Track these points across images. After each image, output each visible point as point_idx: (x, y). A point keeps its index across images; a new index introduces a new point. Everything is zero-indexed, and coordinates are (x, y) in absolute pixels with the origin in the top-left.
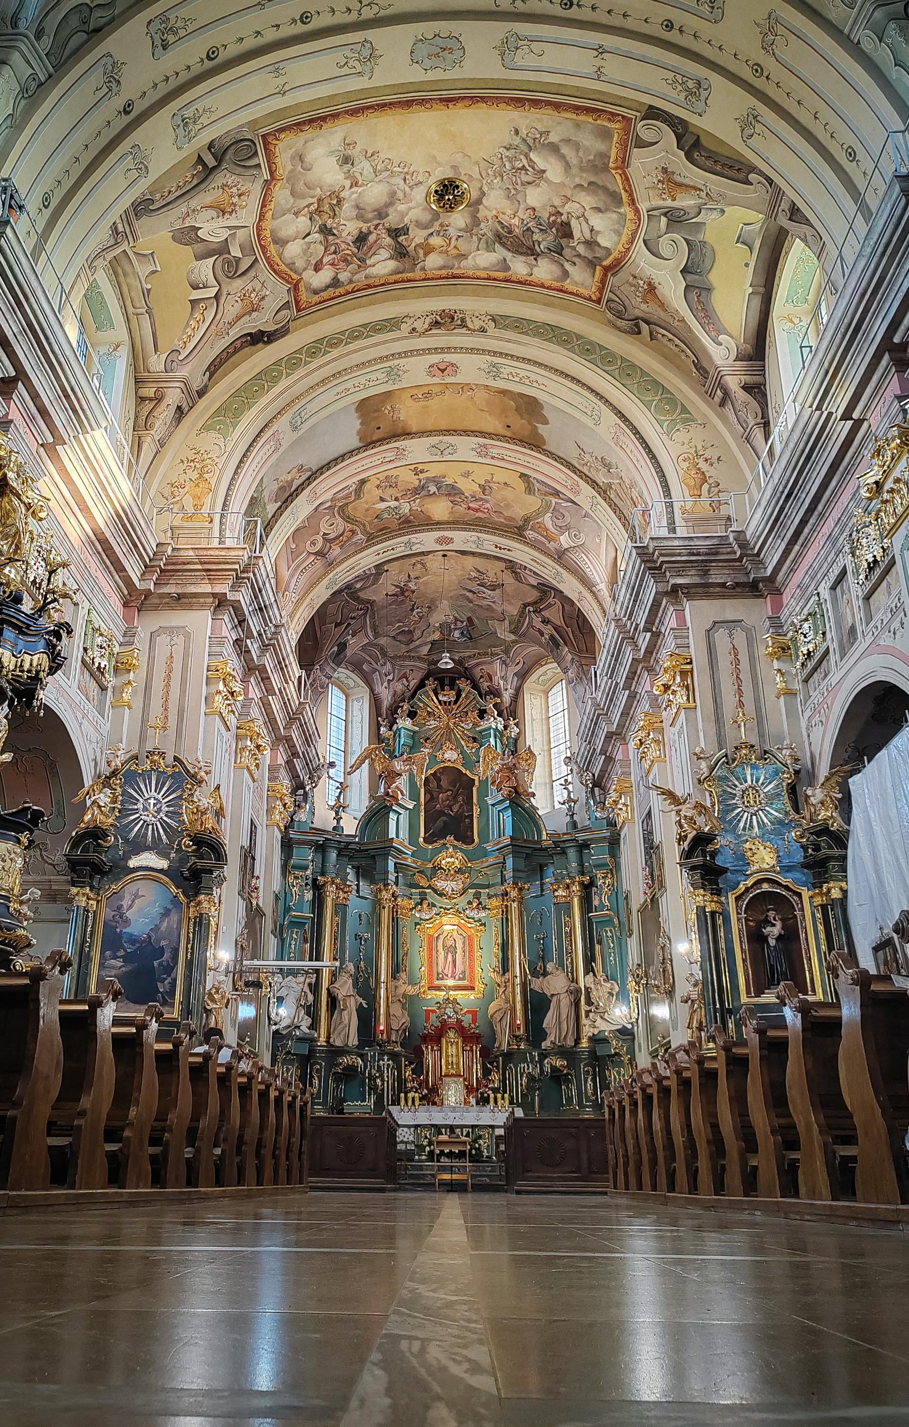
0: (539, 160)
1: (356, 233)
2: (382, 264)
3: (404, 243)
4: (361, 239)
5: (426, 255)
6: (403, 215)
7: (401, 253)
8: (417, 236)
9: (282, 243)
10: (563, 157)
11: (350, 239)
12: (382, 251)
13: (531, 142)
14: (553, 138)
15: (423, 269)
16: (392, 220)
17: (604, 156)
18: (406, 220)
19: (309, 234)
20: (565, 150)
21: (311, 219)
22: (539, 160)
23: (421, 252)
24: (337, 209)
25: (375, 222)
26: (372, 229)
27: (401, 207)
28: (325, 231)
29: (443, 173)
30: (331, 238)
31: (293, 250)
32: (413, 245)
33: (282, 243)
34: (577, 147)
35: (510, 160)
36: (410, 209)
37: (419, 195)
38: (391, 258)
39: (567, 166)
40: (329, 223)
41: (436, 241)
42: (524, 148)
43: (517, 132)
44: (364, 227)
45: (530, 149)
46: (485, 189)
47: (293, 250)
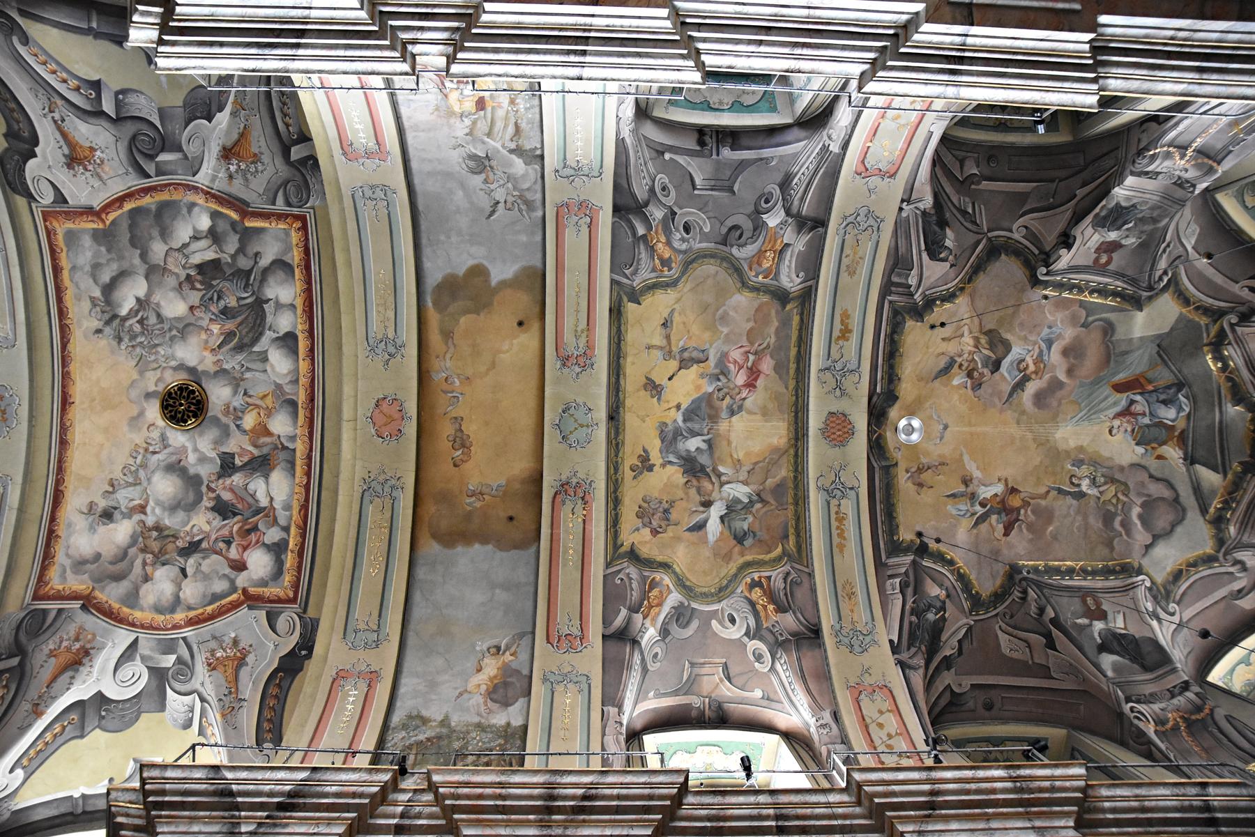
3: (246, 459)
4: (223, 510)
7: (261, 465)
8: (238, 444)
11: (217, 522)
12: (251, 487)
13: (107, 316)
14: (97, 293)
15: (293, 438)
16: (206, 471)
19: (183, 571)
20: (106, 277)
21: (164, 564)
24: (166, 533)
25: (204, 489)
26: (212, 495)
27: (192, 458)
28: (193, 548)
30: (204, 545)
32: (251, 448)
34: (96, 267)
35: (133, 337)
36: (196, 450)
37: (178, 438)
38: (267, 477)
40: (180, 544)
41: (249, 421)
44: (207, 503)
45: (115, 316)
46: (173, 363)
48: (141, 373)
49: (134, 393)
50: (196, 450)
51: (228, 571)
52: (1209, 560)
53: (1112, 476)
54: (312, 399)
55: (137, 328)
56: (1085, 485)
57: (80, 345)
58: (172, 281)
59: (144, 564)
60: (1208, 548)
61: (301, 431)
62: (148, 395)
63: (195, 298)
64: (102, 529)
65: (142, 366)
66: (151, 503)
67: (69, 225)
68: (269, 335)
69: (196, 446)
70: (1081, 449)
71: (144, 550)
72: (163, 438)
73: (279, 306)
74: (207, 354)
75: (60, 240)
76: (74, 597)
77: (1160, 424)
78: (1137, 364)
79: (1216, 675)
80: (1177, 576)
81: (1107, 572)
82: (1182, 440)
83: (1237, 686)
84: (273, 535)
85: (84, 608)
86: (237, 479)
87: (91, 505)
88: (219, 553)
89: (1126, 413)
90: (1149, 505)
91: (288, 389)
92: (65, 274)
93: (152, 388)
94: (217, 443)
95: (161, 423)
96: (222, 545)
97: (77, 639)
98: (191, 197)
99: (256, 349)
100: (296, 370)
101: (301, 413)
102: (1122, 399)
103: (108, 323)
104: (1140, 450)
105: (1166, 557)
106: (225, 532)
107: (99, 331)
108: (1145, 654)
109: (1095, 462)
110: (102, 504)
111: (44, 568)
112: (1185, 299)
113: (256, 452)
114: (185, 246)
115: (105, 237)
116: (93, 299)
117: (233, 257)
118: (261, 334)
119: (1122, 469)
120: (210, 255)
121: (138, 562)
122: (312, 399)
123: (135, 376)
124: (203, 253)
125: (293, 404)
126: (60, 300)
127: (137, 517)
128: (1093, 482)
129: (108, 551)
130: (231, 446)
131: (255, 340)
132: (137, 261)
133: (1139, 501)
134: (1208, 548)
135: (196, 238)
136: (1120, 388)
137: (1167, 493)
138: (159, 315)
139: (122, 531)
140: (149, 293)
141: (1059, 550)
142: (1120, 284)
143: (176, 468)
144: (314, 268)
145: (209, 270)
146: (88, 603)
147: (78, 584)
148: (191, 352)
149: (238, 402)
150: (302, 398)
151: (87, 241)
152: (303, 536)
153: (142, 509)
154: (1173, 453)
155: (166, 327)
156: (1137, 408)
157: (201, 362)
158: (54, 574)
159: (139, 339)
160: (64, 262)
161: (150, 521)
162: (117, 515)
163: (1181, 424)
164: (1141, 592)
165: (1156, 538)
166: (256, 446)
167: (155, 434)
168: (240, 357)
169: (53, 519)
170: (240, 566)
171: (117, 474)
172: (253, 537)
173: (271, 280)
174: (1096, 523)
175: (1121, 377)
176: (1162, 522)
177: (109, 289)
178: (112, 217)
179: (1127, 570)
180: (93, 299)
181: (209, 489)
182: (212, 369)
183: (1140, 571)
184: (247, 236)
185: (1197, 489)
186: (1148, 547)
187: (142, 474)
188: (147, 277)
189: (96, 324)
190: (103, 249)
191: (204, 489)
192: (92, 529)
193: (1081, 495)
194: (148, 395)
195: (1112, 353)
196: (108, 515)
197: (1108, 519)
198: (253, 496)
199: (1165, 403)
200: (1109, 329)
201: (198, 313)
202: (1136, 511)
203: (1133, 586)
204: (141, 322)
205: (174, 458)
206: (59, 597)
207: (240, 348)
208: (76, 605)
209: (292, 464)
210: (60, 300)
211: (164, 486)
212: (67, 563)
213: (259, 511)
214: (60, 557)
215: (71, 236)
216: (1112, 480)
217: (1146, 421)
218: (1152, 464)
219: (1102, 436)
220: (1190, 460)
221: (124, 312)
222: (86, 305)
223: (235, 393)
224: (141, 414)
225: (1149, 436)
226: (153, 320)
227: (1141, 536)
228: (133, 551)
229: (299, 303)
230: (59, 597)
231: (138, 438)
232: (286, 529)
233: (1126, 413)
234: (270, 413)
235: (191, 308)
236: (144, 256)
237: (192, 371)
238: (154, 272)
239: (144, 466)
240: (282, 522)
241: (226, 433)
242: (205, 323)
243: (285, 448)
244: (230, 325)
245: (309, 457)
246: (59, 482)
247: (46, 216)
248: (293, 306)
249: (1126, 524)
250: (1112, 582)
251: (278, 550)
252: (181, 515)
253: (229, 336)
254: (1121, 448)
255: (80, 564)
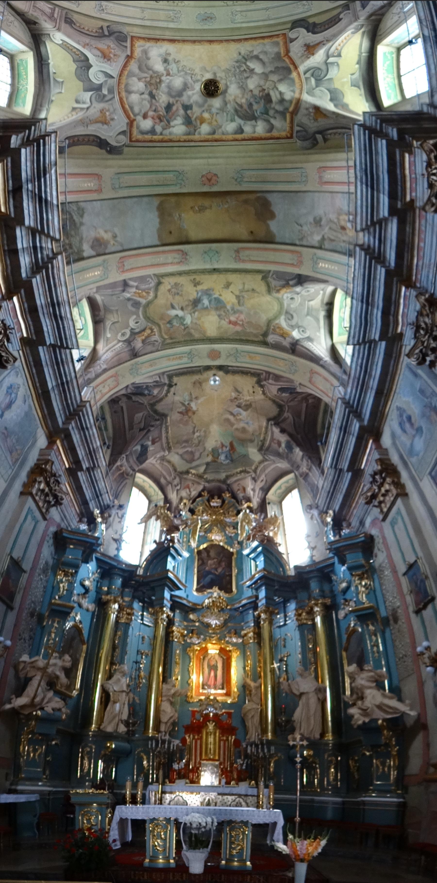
0: (252, 65)
1: (166, 102)
2: (178, 128)
3: (190, 115)
4: (169, 107)
5: (201, 123)
6: (189, 97)
7: (188, 121)
8: (196, 111)
9: (129, 92)
10: (261, 60)
11: (164, 105)
14: (255, 53)
15: (200, 134)
16: (184, 99)
17: (278, 54)
18: (192, 101)
19: (143, 93)
20: (261, 56)
22: (252, 65)
23: (198, 122)
27: (190, 93)
28: (152, 96)
29: (208, 76)
30: (154, 101)
31: (134, 98)
32: (195, 116)
33: (129, 92)
34: (266, 53)
35: (239, 67)
37: (198, 87)
38: (183, 124)
39: (264, 63)
40: (154, 91)
41: (206, 115)
42: (244, 61)
43: (240, 54)
44: (171, 100)
45: (246, 60)
47: (134, 98)
48: (224, 71)
49: (215, 68)
50: (193, 94)
51: (143, 112)
52: (175, 470)
53: (201, 442)
54: (216, 141)
55: (242, 69)
56: (197, 434)
57: (234, 47)
58: (262, 83)
59: (146, 78)
60: (179, 469)
61: (203, 137)
62: (215, 74)
63: (256, 92)
64: (160, 59)
65: (227, 71)
66: (171, 78)
67: (281, 43)
68: (242, 122)
69: (195, 94)
70: (210, 432)
71: (151, 77)
72: (198, 81)
73: (254, 126)
74: (233, 97)
75: (275, 39)
76: (132, 52)
77: (219, 455)
78: (240, 450)
79: (138, 475)
80: (169, 462)
81: (168, 443)
82: (214, 461)
83: (136, 480)
84: (158, 129)
85: (128, 56)
86: (182, 112)
87: (169, 54)
88: (151, 107)
89: (223, 445)
90: (192, 453)
91: (220, 131)
92: (261, 41)
93: (218, 75)
94: (197, 103)
95: (204, 79)
96: (154, 108)
97: (115, 55)
98: (297, 91)
99: (236, 117)
100: (228, 134)
101: (210, 137)
102: (227, 444)
103: (243, 57)
104: (210, 449)
105: (175, 458)
106: (159, 109)
107: (240, 54)
108: (142, 457)
109: (206, 436)
110: (170, 58)
111: (144, 39)
112: (260, 463)
113: (193, 119)
114: (277, 89)
115: (278, 57)
116: (252, 51)
117: (274, 108)
118: (242, 119)
119: (204, 444)
120: (274, 99)
121: (146, 75)
122: (216, 141)
123: (223, 68)
124: (275, 96)
125: (214, 133)
126: (251, 39)
127: (165, 73)
128: (198, 437)
129: (151, 63)
130: (195, 108)
131: (239, 117)
132: (269, 69)
133: (193, 450)
134: (178, 470)
135: (281, 93)
136: (231, 444)
137: (196, 458)
138: (248, 78)
139: (159, 67)
140: (256, 74)
141: (174, 426)
142: (267, 443)
143: (186, 87)
144: (271, 141)
145: (267, 99)
146: (129, 58)
147: (138, 52)
148: (233, 91)
149: (214, 110)
150: (216, 136)
151: (276, 50)
152: (159, 141)
153: (168, 74)
154: (209, 459)
155: (243, 80)
156: (224, 449)
157: (230, 95)
158: (141, 43)
159: (238, 70)
160: (266, 41)
161: (164, 78)
162: (165, 65)
163: (219, 461)
164: (162, 453)
165: (181, 456)
166: (196, 119)
167: (199, 77)
168: (232, 111)
169: (164, 40)
170: (145, 117)
171: (182, 63)
172: (157, 121)
173: (265, 123)
174: (185, 438)
175: (235, 444)
176: (186, 456)
177: (257, 57)
178: (287, 60)
179: (169, 449)
180: (252, 51)
181: (177, 101)
182: (227, 100)
183: (169, 452)
184: (283, 114)
185: (198, 466)
186: (178, 454)
187: (182, 73)
188: (263, 73)
189: (243, 52)
190: (273, 56)
191: (177, 98)
192: (160, 55)
193: (194, 433)
194: (215, 74)
195: (243, 442)
196: (165, 61)
197: (186, 441)
198: (175, 119)
199: (226, 457)
200: (252, 441)
201: (250, 93)
202: (190, 449)
203: (164, 451)
204: (245, 70)
205: (189, 85)
206: (132, 46)
207: (236, 111)
208: (129, 53)
209: (189, 134)
210: (251, 39)
211: (178, 82)
212: (146, 47)
213: (169, 122)
214: (148, 44)
215: (277, 44)
216: (199, 442)
217: (220, 451)
218: (206, 453)
219: (215, 437)
220: (208, 464)
221: (248, 63)
222: (250, 49)
223: (218, 109)
224: (208, 71)
225: (215, 452)
226: (246, 75)
227: (181, 451)
228: (151, 72)
229: (256, 135)
230: (132, 46)
231: (197, 71)
232: (161, 134)
233: (223, 445)
234: (210, 124)
235: (251, 91)
236: (271, 72)
237: (225, 91)
238: (265, 76)
239: (186, 73)
240: (165, 132)
241: (200, 106)
242: (246, 96)
243: (195, 130)
244: (245, 107)
245: (192, 141)
246: (179, 41)
247: (284, 34)
248: (254, 132)
249: (185, 447)
250: (165, 445)
251: (153, 131)
252: (166, 90)
253: (241, 106)
254: (211, 444)
255: (145, 52)
